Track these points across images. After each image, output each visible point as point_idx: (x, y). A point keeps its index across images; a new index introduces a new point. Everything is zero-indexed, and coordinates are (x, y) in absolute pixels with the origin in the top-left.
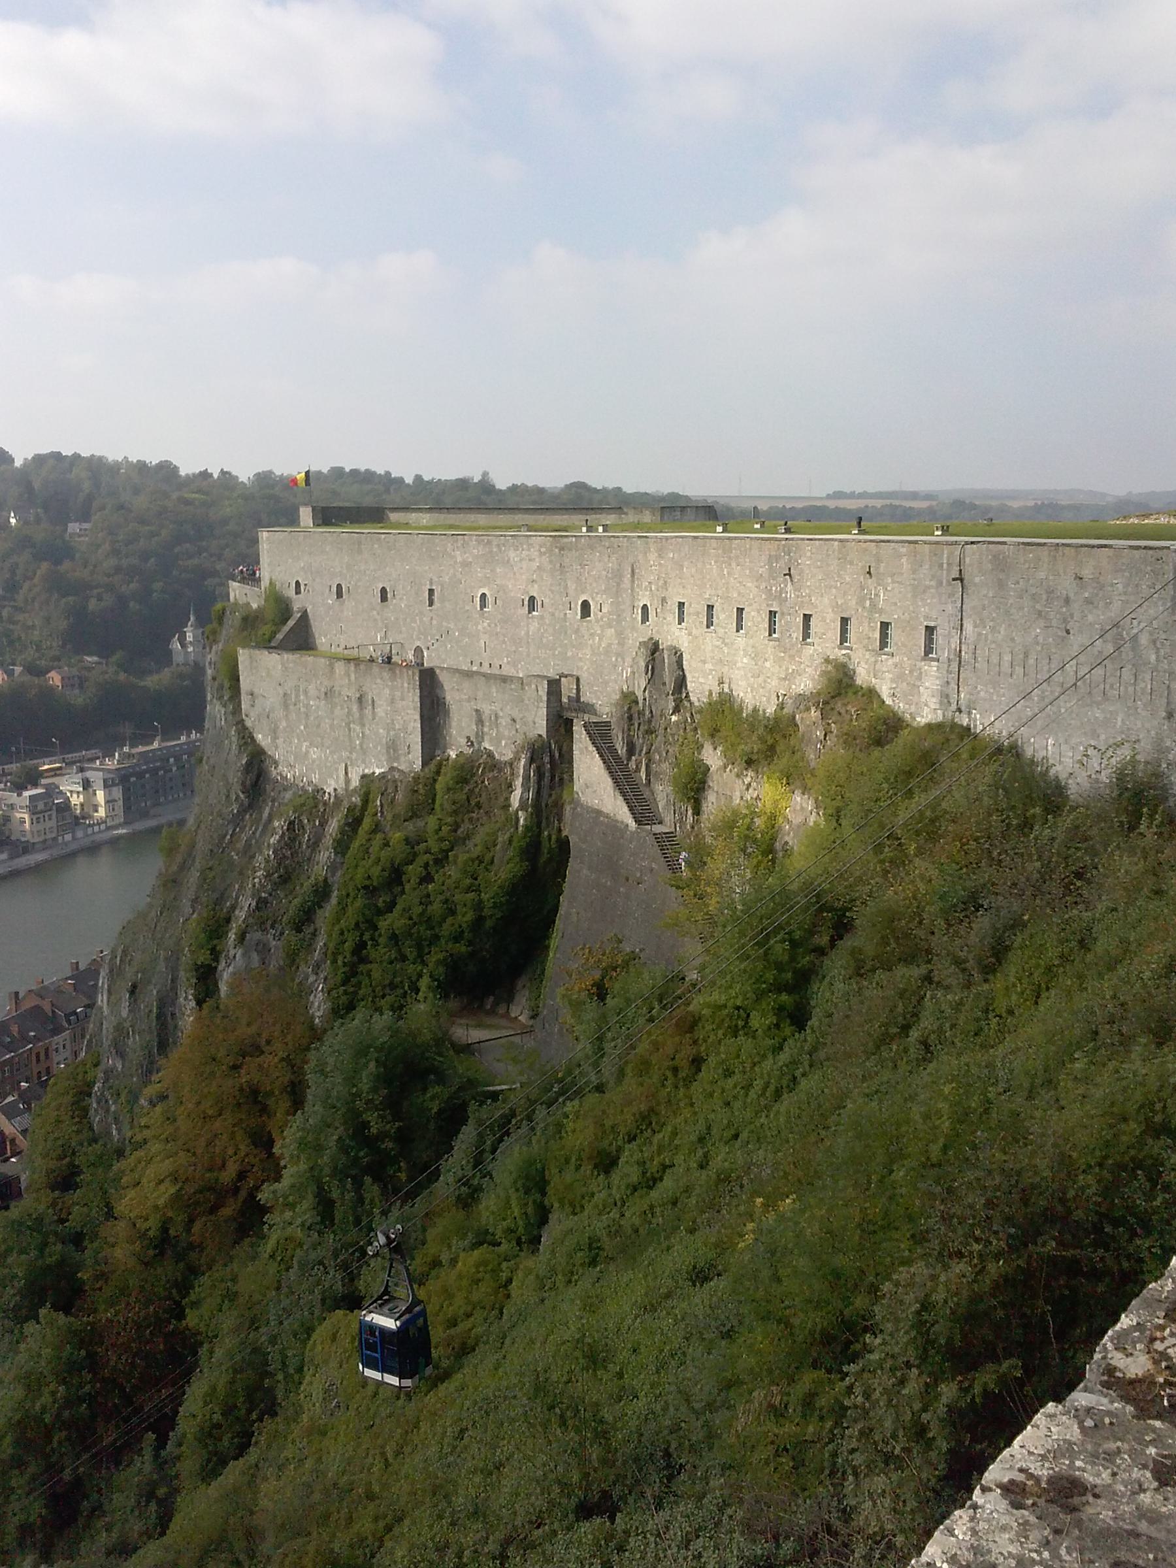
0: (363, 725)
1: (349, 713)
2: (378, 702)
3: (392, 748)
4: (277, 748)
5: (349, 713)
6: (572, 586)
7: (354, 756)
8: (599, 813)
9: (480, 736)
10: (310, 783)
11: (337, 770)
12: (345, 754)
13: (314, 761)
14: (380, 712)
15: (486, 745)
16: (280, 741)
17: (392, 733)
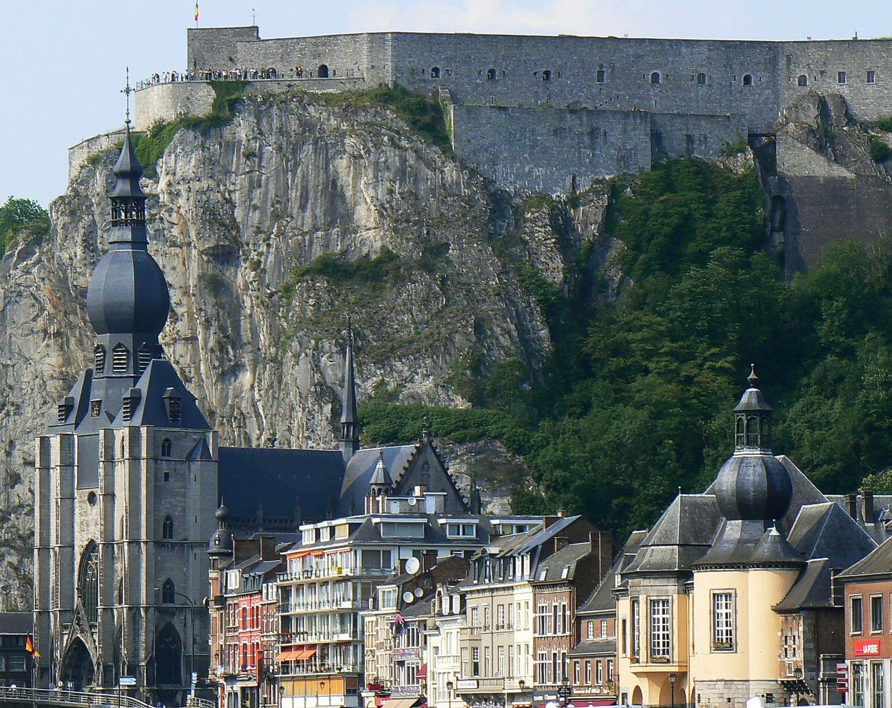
3: (623, 160)
11: (564, 180)
13: (538, 177)
16: (499, 167)
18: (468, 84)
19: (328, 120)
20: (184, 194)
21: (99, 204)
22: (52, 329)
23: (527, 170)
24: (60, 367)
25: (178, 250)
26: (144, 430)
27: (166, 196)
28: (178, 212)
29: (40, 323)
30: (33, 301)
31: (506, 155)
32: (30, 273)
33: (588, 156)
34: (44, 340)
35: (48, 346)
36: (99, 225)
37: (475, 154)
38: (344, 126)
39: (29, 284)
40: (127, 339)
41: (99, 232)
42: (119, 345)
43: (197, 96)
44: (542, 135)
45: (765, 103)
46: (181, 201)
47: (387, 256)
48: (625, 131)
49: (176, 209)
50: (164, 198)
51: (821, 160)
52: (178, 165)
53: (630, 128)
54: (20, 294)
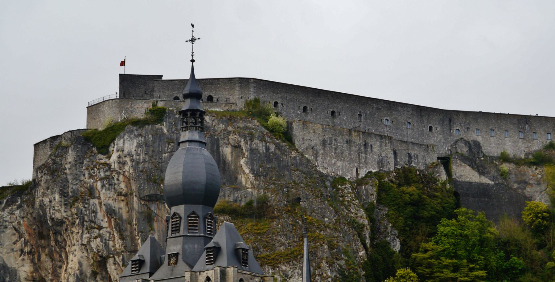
0: (366, 154)
1: (359, 149)
2: (374, 146)
3: (381, 163)
4: (317, 161)
5: (359, 149)
6: (425, 121)
7: (361, 165)
8: (470, 183)
9: (410, 162)
10: (337, 175)
11: (352, 170)
12: (356, 164)
13: (339, 167)
14: (375, 150)
15: (413, 164)
16: (319, 158)
17: (381, 157)
18: (294, 113)
19: (219, 124)
20: (129, 163)
21: (70, 169)
22: (26, 249)
23: (333, 162)
24: (32, 273)
25: (123, 198)
26: (231, 271)
27: (116, 165)
28: (123, 175)
29: (18, 245)
30: (14, 232)
31: (322, 152)
32: (14, 214)
33: (363, 158)
34: (20, 256)
35: (23, 260)
36: (70, 181)
37: (307, 149)
38: (230, 128)
39: (12, 220)
40: (199, 209)
41: (71, 186)
42: (194, 213)
43: (135, 107)
44: (340, 143)
45: (440, 142)
46: (127, 168)
47: (263, 203)
48: (381, 146)
49: (122, 173)
50: (115, 166)
51: (476, 174)
52: (127, 144)
53: (383, 144)
54: (6, 227)
